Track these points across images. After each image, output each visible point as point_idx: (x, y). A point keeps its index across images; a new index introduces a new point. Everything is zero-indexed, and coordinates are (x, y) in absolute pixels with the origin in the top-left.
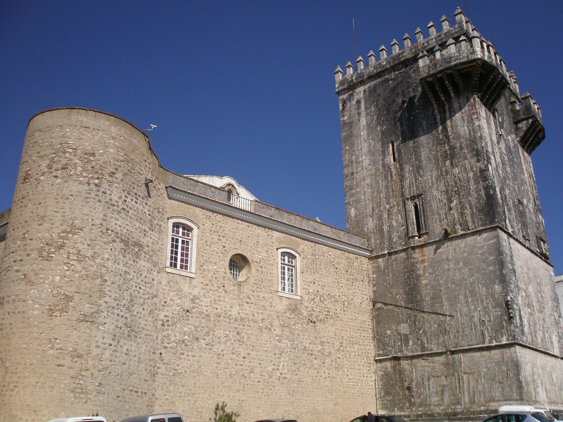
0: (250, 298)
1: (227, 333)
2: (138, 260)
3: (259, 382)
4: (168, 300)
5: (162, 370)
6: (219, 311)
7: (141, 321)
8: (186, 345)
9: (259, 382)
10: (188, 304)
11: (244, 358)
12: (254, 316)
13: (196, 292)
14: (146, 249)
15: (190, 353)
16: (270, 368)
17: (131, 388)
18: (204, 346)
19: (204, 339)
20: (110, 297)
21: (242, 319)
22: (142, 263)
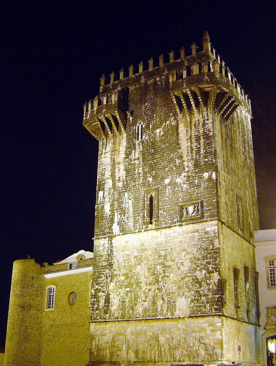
0: (76, 313)
1: (65, 332)
2: (29, 312)
3: (77, 353)
4: (46, 323)
5: (43, 352)
6: (63, 323)
7: (32, 335)
8: (51, 341)
9: (77, 353)
10: (52, 323)
11: (72, 342)
12: (77, 321)
13: (54, 317)
14: (34, 306)
15: (52, 344)
16: (82, 346)
17: (27, 361)
18: (57, 340)
19: (57, 337)
20: (16, 329)
21: (72, 324)
22: (32, 312)
